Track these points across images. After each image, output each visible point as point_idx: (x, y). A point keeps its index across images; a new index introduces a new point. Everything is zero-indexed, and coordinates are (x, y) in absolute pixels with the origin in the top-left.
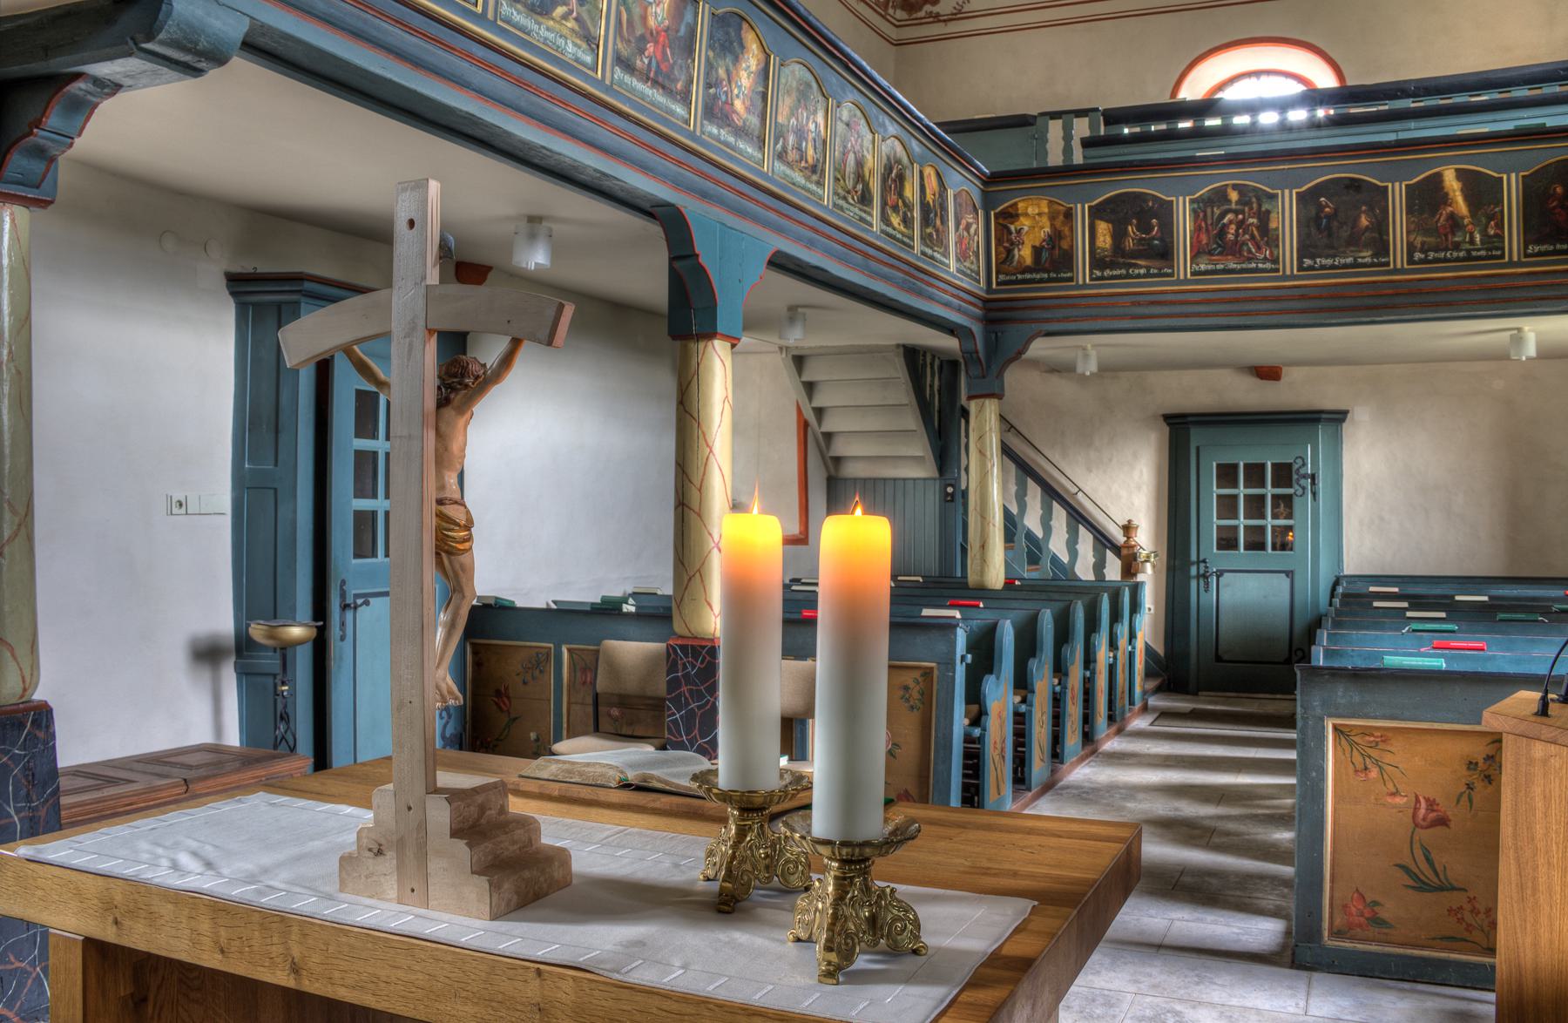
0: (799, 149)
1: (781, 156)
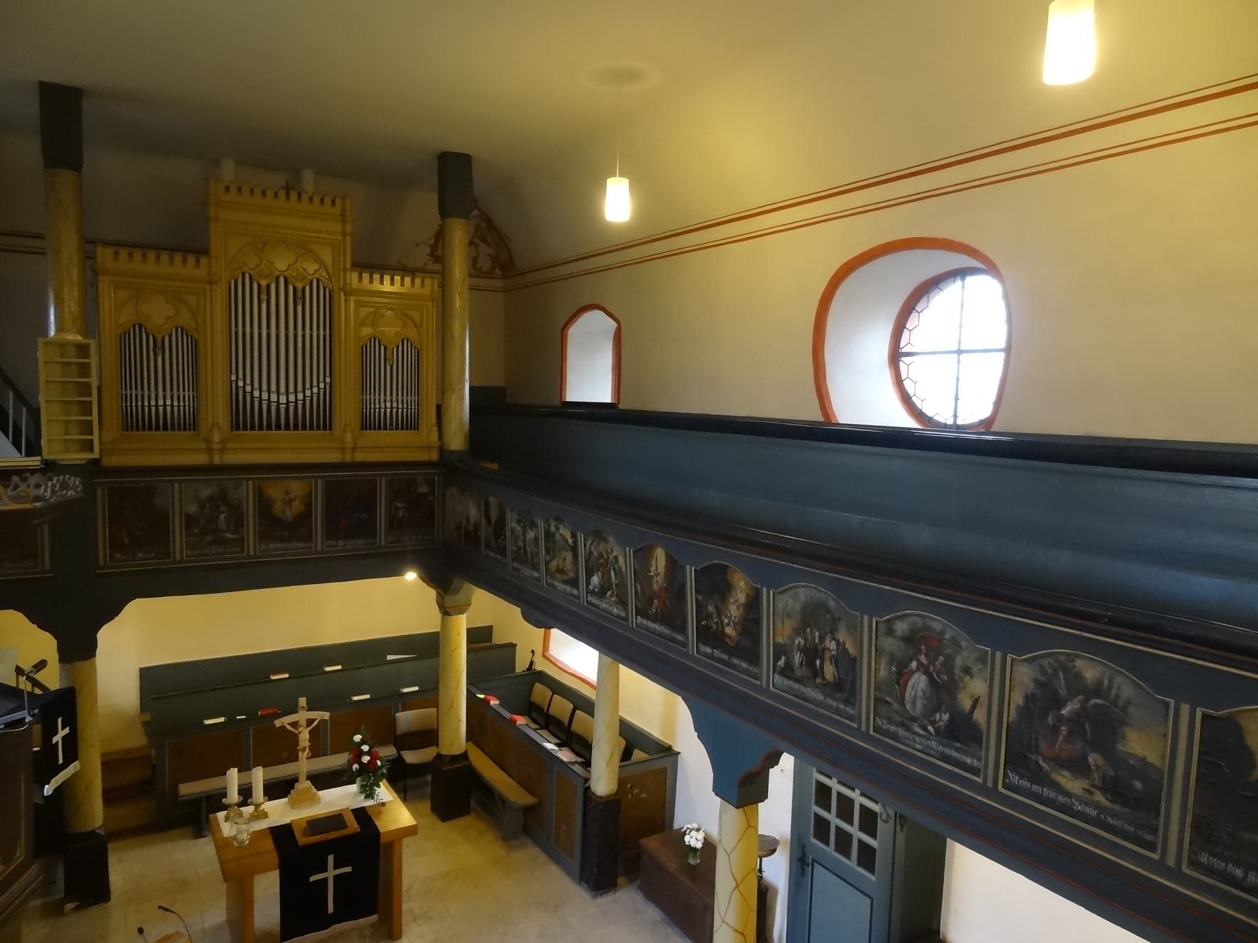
0: (811, 665)
1: (787, 672)
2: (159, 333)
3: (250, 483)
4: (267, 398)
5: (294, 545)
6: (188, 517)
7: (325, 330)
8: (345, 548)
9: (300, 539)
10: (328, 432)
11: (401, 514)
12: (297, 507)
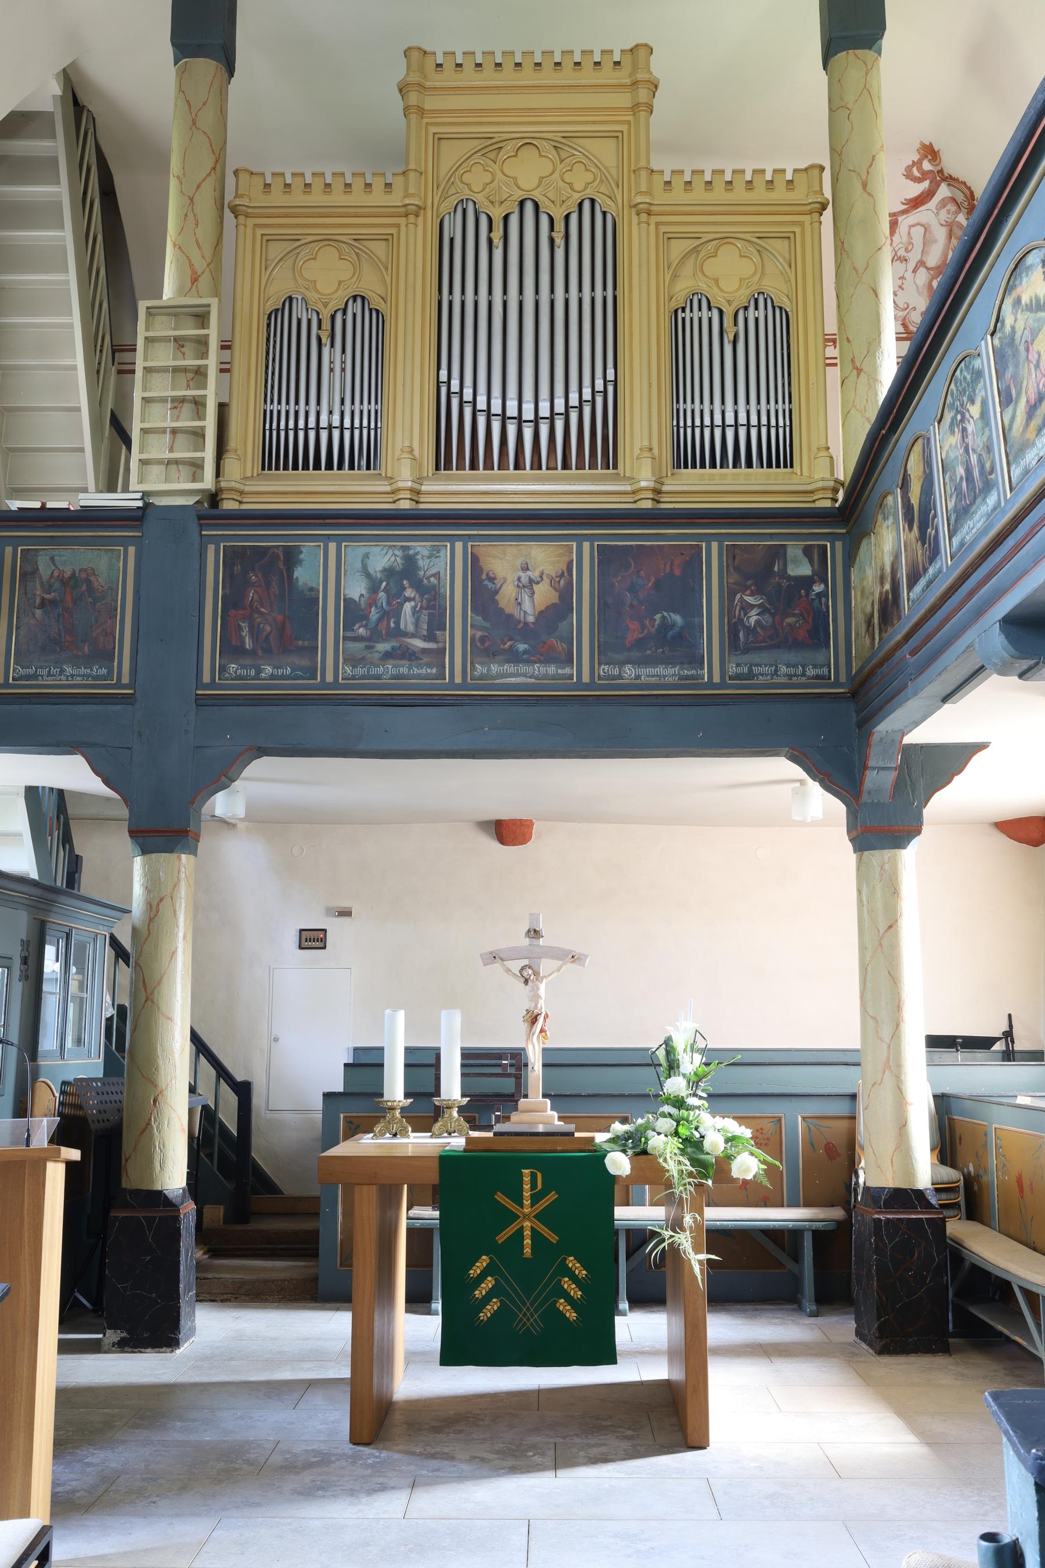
2: (326, 305)
3: (459, 545)
4: (500, 412)
5: (538, 669)
6: (348, 601)
7: (605, 289)
8: (638, 681)
9: (548, 657)
10: (611, 471)
11: (753, 620)
12: (544, 595)
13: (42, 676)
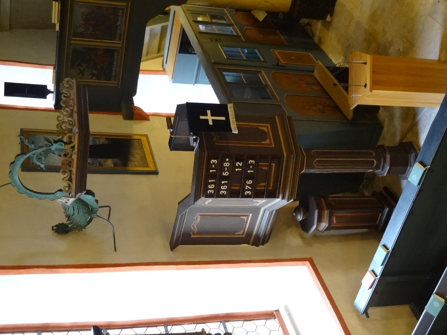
13: (120, 32)
